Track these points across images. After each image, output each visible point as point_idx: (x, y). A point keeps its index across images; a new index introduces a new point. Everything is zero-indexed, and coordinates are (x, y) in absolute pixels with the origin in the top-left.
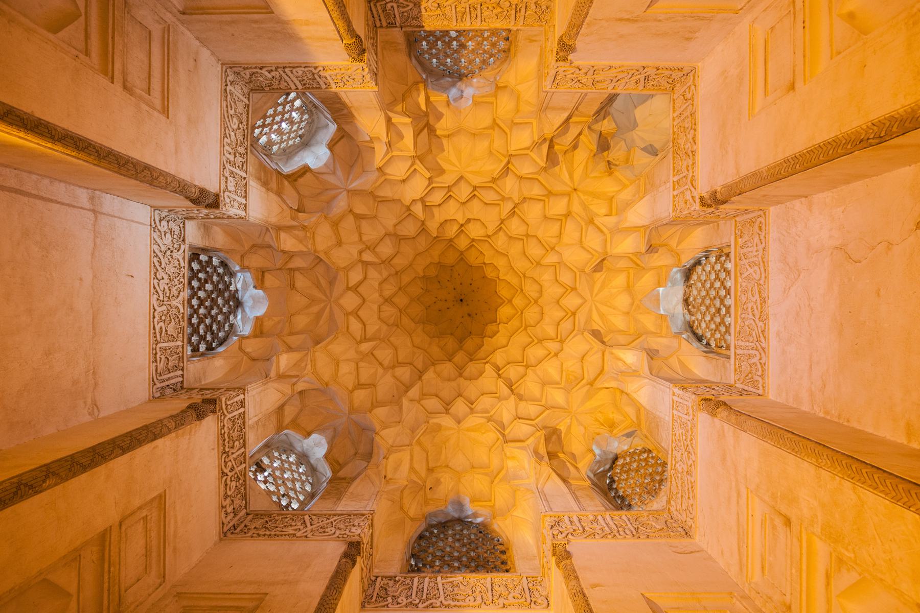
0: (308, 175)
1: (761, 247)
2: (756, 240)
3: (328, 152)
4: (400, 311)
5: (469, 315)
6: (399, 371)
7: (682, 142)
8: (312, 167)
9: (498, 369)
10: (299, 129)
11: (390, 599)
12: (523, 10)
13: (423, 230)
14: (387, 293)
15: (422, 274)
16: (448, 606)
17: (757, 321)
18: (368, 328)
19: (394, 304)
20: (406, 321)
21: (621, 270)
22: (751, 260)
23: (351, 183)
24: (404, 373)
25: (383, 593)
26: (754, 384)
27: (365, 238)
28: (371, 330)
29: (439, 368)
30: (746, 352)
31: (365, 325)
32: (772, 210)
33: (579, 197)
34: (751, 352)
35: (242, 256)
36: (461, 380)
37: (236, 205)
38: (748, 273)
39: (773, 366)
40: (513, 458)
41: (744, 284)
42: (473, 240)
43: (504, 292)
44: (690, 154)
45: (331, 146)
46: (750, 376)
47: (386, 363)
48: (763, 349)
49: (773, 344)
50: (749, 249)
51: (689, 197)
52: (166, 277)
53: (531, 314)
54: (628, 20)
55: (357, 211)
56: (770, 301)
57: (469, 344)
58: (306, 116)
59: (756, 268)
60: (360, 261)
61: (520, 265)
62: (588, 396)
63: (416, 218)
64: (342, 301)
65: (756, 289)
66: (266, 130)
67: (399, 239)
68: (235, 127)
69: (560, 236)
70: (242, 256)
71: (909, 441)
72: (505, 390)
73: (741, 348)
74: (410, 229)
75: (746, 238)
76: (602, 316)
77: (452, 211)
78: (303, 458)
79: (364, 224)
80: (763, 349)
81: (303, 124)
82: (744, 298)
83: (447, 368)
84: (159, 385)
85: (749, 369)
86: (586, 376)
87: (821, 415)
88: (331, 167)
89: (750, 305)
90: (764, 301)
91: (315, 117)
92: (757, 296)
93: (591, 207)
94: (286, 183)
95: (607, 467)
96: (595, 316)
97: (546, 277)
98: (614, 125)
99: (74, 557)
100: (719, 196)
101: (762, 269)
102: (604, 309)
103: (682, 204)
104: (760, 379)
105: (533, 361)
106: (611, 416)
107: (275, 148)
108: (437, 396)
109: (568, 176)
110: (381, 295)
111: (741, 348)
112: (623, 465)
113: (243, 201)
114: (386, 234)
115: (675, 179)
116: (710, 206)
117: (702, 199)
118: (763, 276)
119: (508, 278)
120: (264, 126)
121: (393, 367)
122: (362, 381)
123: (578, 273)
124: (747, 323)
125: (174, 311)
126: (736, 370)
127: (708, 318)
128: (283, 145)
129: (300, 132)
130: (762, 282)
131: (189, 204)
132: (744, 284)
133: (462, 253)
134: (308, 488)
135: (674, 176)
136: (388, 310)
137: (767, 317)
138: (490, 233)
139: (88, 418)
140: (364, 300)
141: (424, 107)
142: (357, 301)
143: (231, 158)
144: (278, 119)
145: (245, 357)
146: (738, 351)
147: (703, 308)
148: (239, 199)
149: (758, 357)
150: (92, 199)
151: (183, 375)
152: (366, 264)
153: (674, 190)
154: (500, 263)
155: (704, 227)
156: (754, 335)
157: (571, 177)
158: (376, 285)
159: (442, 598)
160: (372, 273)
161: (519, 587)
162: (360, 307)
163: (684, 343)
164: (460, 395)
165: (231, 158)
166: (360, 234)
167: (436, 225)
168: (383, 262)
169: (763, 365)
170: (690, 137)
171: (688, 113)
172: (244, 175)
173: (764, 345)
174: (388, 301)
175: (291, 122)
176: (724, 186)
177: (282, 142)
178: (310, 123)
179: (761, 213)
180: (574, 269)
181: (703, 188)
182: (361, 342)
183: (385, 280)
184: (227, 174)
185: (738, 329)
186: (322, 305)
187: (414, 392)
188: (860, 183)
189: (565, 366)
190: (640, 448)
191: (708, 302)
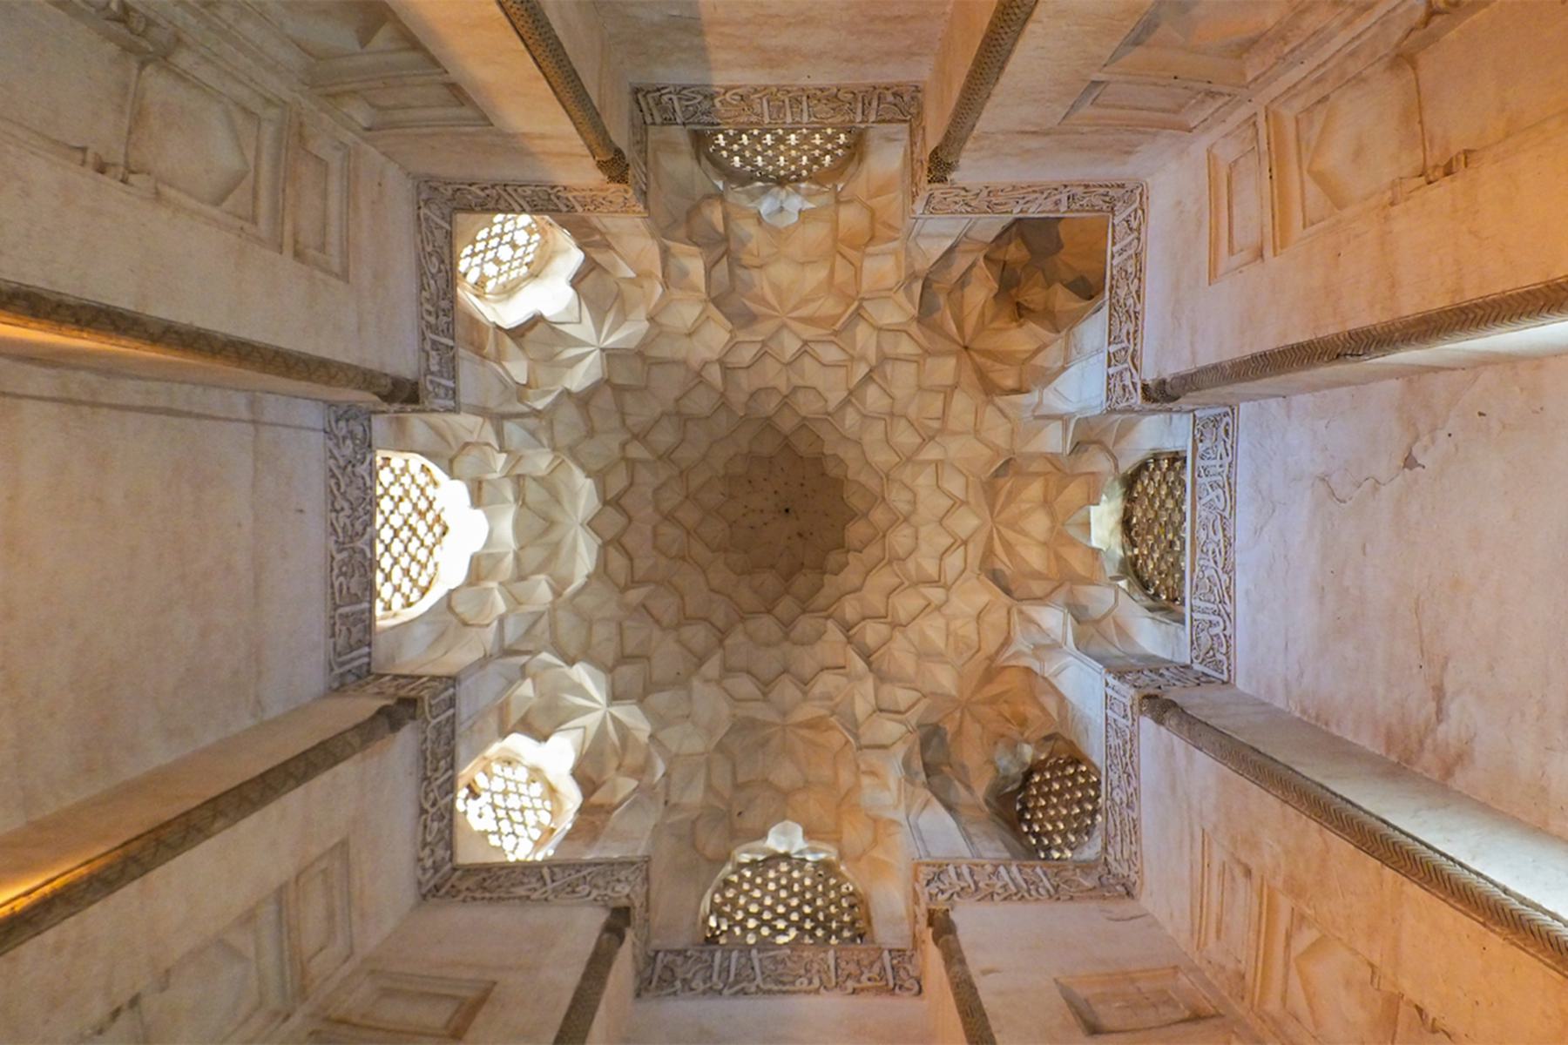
0: (540, 326)
2: (1221, 449)
3: (571, 291)
4: (688, 533)
5: (800, 535)
6: (687, 632)
7: (1122, 293)
8: (547, 314)
9: (846, 628)
10: (526, 254)
11: (678, 984)
12: (875, 104)
13: (724, 403)
14: (666, 506)
15: (722, 472)
16: (769, 992)
18: (637, 562)
19: (678, 523)
20: (698, 549)
21: (1038, 474)
24: (698, 635)
25: (667, 975)
26: (1217, 666)
27: (630, 421)
28: (642, 566)
29: (752, 625)
31: (631, 559)
32: (1245, 408)
33: (972, 359)
36: (786, 646)
37: (442, 392)
39: (1241, 642)
41: (1204, 514)
42: (804, 418)
43: (856, 502)
45: (576, 282)
47: (666, 620)
51: (1128, 382)
52: (346, 505)
54: (1034, 133)
55: (618, 380)
57: (801, 583)
58: (536, 237)
60: (624, 459)
61: (882, 457)
63: (710, 387)
65: (1218, 523)
66: (477, 260)
67: (683, 419)
68: (434, 271)
69: (943, 417)
71: (1388, 750)
72: (859, 664)
74: (701, 403)
76: (1008, 547)
77: (772, 374)
78: (536, 773)
79: (629, 399)
81: (531, 249)
82: (1202, 535)
83: (766, 626)
84: (337, 671)
87: (1298, 714)
88: (576, 313)
89: (1211, 547)
90: (1229, 544)
91: (549, 236)
93: (991, 375)
94: (508, 341)
95: (1016, 786)
97: (924, 481)
98: (1025, 252)
99: (248, 918)
100: (1168, 390)
102: (1010, 535)
103: (1119, 390)
105: (903, 616)
106: (1021, 708)
107: (490, 285)
108: (749, 672)
110: (657, 509)
112: (1039, 785)
113: (450, 384)
114: (663, 414)
116: (1155, 401)
119: (863, 478)
120: (473, 254)
121: (678, 626)
122: (628, 651)
125: (358, 557)
128: (503, 279)
129: (528, 259)
131: (376, 398)
133: (786, 437)
134: (545, 818)
136: (669, 532)
137: (1233, 569)
138: (830, 409)
139: (249, 722)
140: (630, 519)
141: (721, 229)
142: (620, 520)
143: (432, 319)
144: (493, 243)
148: (444, 382)
150: (252, 404)
151: (369, 655)
152: (631, 464)
154: (849, 454)
157: (960, 328)
158: (649, 495)
159: (759, 980)
160: (644, 475)
162: (625, 530)
163: (1122, 596)
164: (785, 671)
165: (432, 319)
166: (623, 415)
167: (743, 398)
168: (660, 458)
170: (1133, 288)
172: (451, 343)
174: (669, 517)
175: (514, 246)
177: (500, 274)
178: (543, 244)
182: (624, 589)
183: (664, 484)
184: (428, 347)
187: (712, 667)
188: (1345, 389)
189: (952, 627)
190: (1064, 756)
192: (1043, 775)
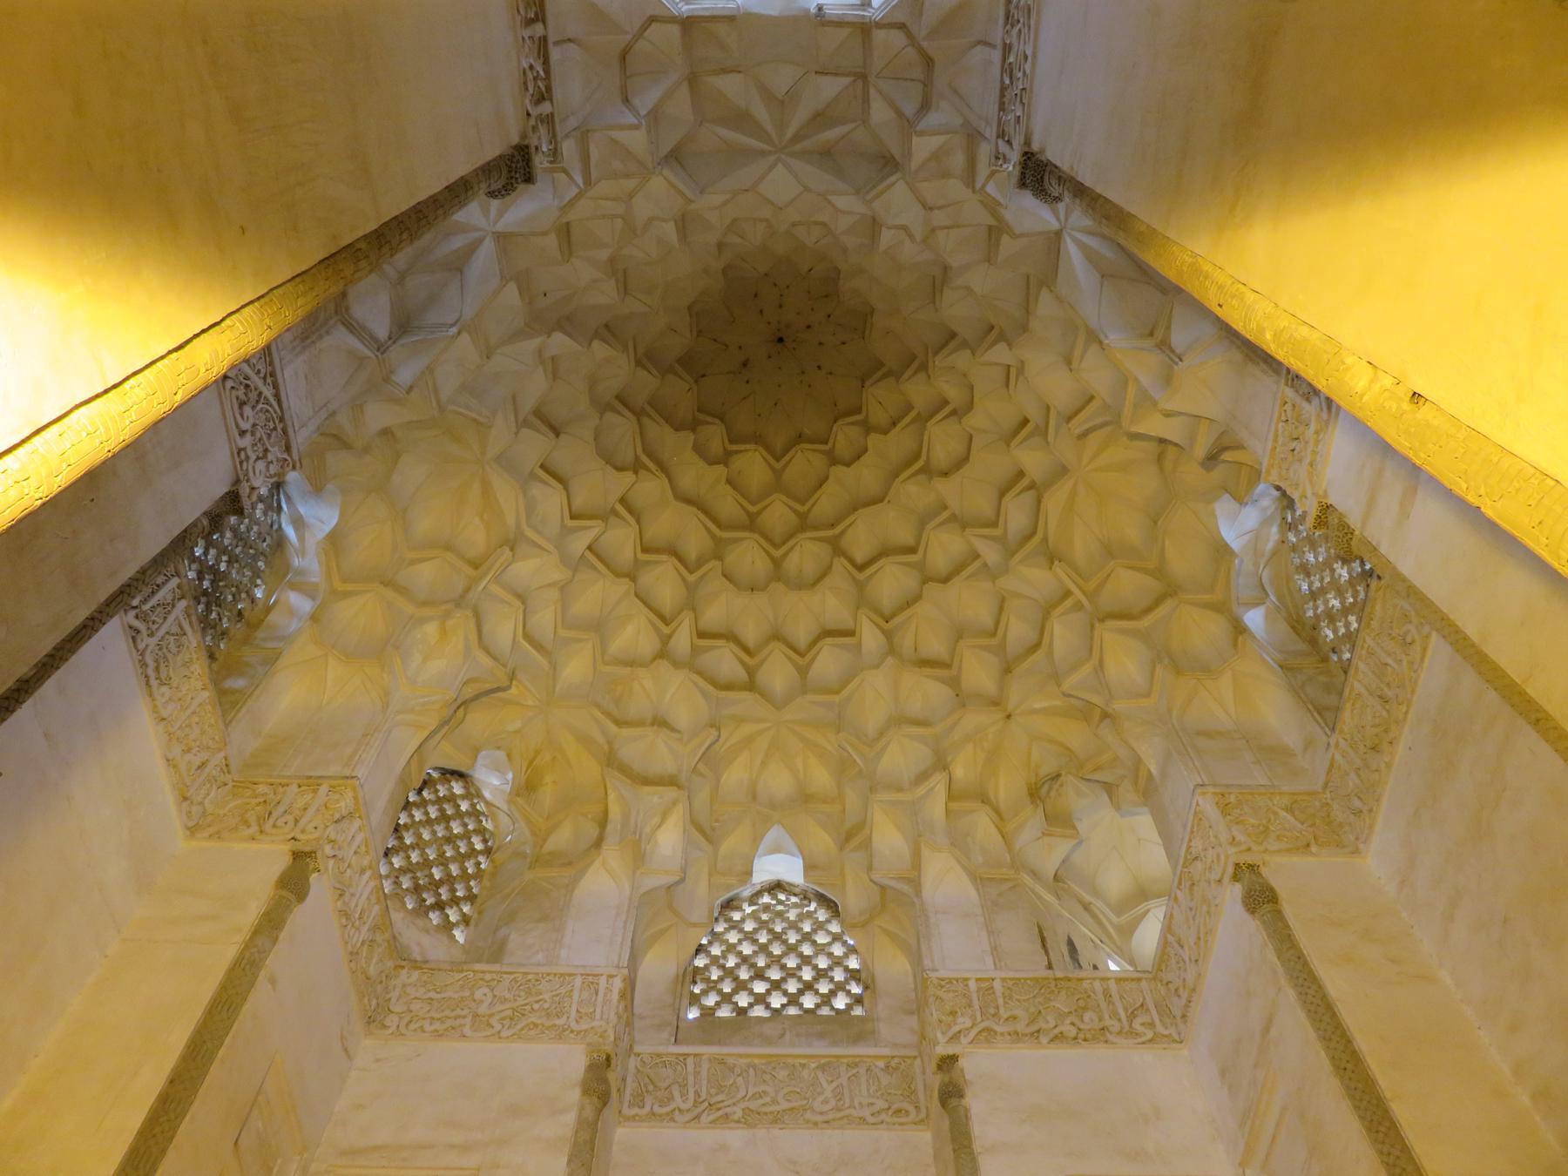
1: (866, 1113)
16: (144, 665)
17: (743, 1105)
22: (846, 1091)
23: (1075, 240)
30: (691, 1079)
34: (691, 1094)
35: (902, 26)
38: (825, 1084)
40: (444, 632)
44: (1034, 1028)
46: (651, 1088)
48: (697, 1117)
49: (707, 1137)
50: (864, 1088)
53: (749, 556)
56: (776, 1132)
59: (833, 1102)
62: (584, 740)
64: (780, 167)
70: (902, 26)
73: (697, 1065)
75: (885, 1080)
76: (748, 741)
80: (697, 1117)
85: (663, 1085)
86: (625, 732)
92: (786, 1105)
96: (747, 729)
100: (953, 1102)
101: (830, 1116)
104: (647, 1109)
106: (548, 779)
109: (1037, 706)
111: (697, 1065)
112: (452, 799)
115: (997, 985)
117: (953, 1058)
118: (819, 1118)
123: (837, 698)
124: (740, 1080)
126: (659, 1055)
127: (747, 949)
130: (808, 1115)
132: (805, 1073)
135: (1003, 980)
145: (629, 37)
146: (690, 1061)
147: (763, 938)
149: (684, 1107)
153: (978, 980)
155: (911, 979)
156: (720, 1097)
161: (204, 756)
169: (670, 1117)
171: (1108, 1022)
173: (704, 1118)
176: (967, 1110)
179: (923, 1115)
180: (846, 692)
181: (976, 1063)
185: (731, 1061)
186: (769, 127)
191: (776, 950)
192: (463, 797)
